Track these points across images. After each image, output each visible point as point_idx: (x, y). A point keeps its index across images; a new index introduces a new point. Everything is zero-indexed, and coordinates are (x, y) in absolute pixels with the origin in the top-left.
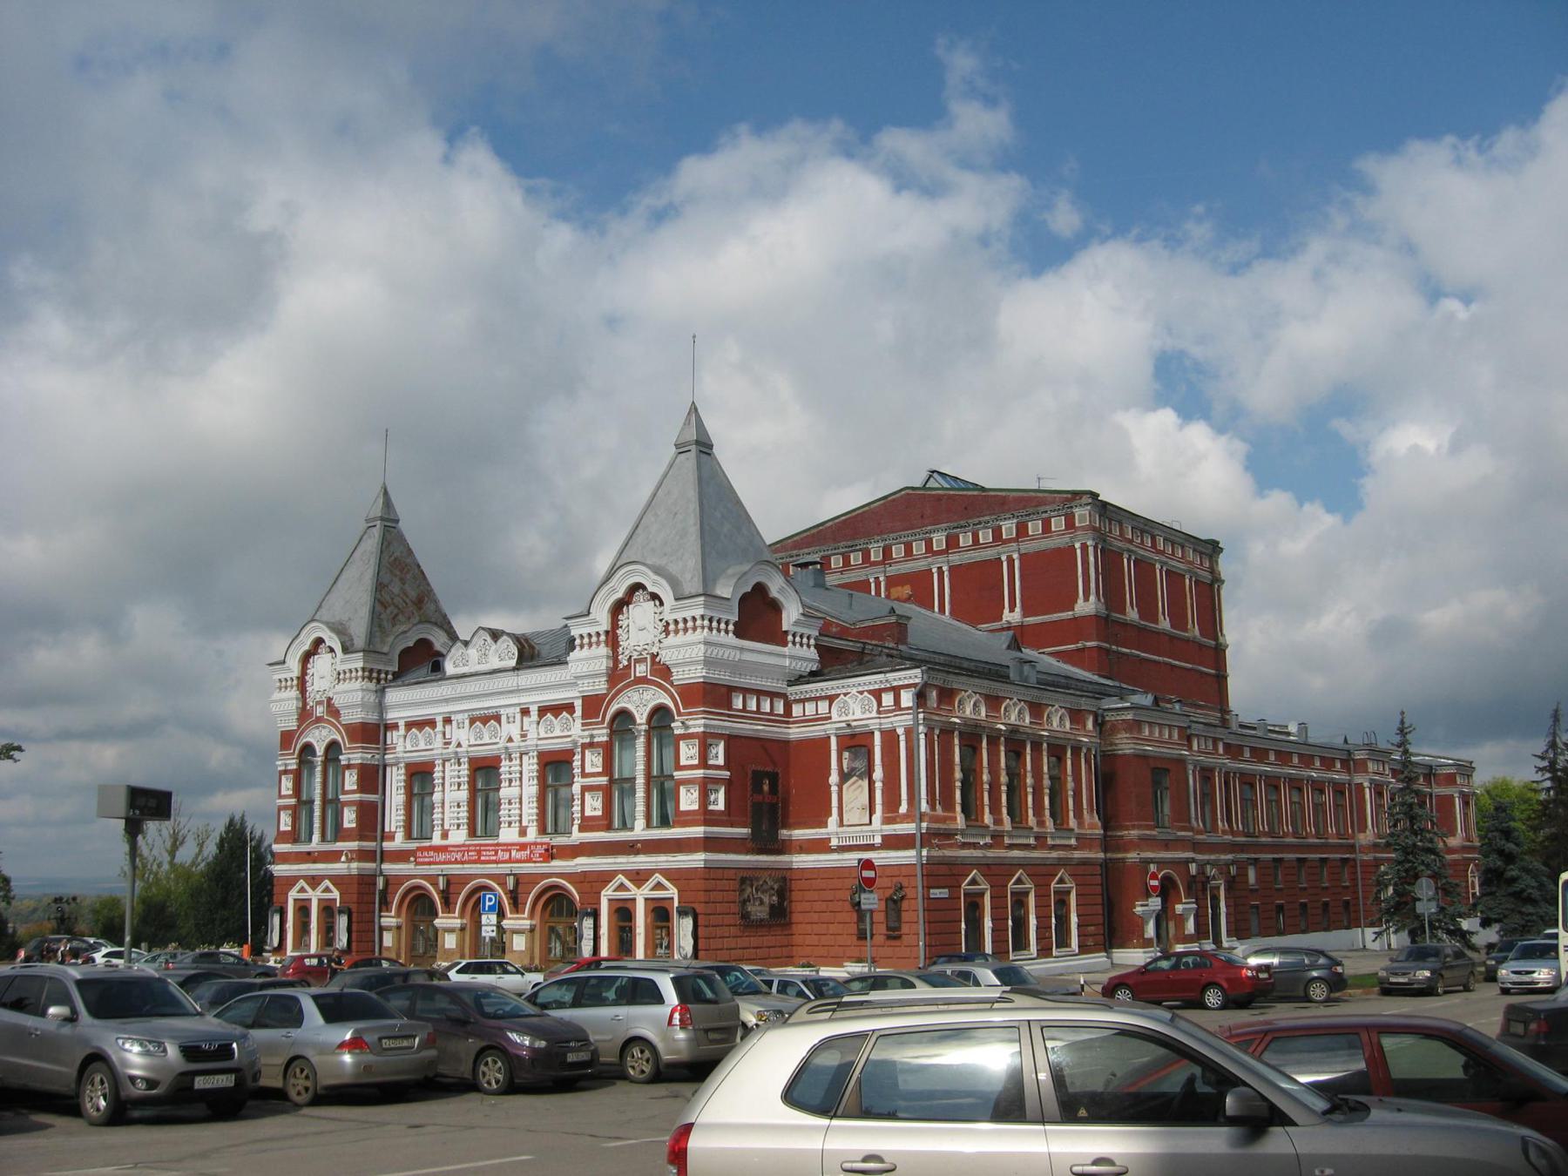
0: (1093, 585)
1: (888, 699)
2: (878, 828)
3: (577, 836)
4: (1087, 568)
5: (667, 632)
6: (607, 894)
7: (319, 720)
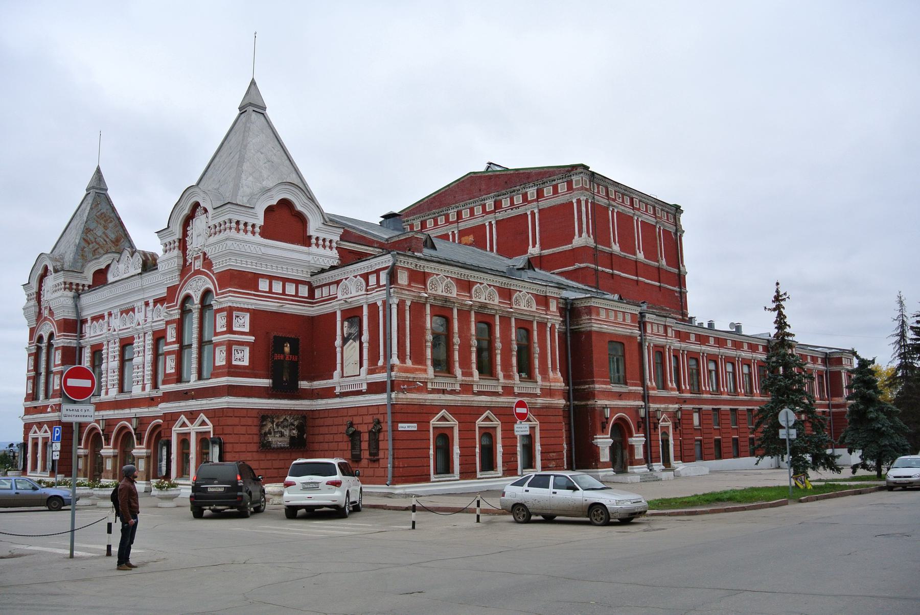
0: (584, 226)
1: (372, 279)
2: (364, 378)
4: (583, 218)
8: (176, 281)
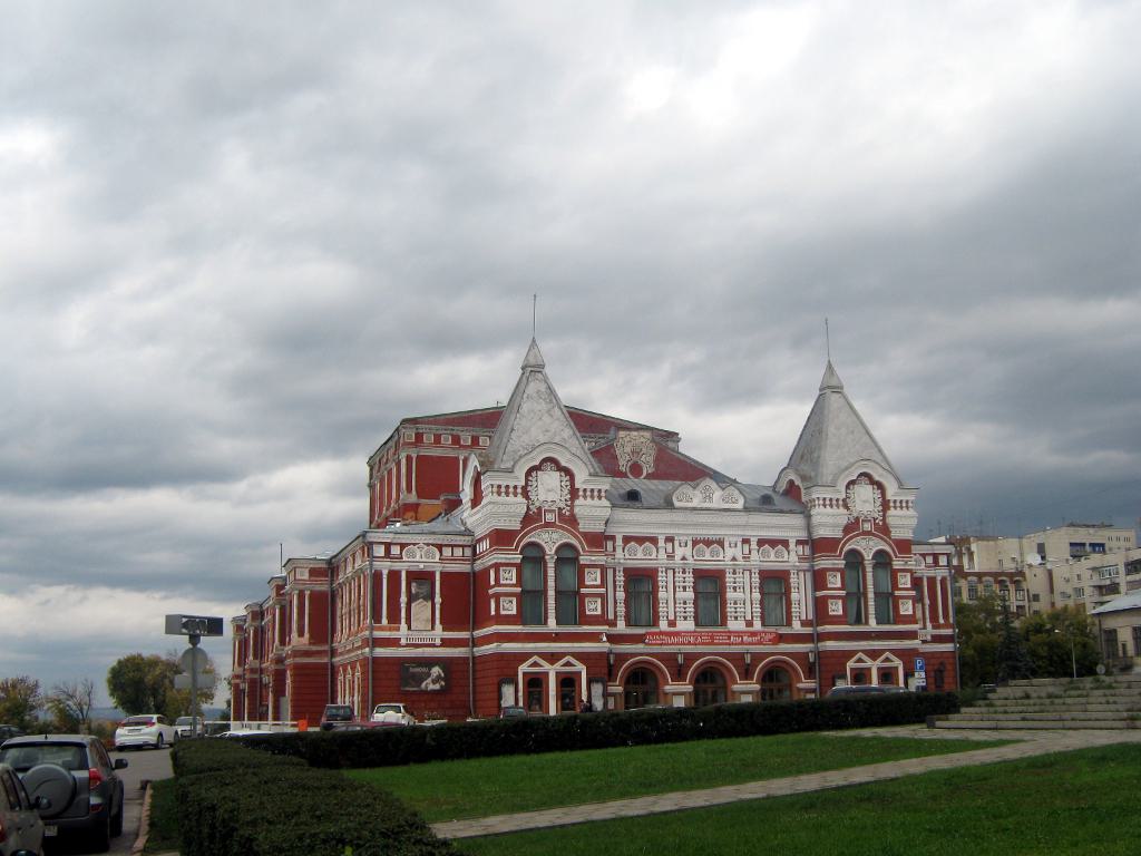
3: (797, 627)
5: (885, 505)
6: (850, 664)
7: (548, 525)
8: (839, 534)
